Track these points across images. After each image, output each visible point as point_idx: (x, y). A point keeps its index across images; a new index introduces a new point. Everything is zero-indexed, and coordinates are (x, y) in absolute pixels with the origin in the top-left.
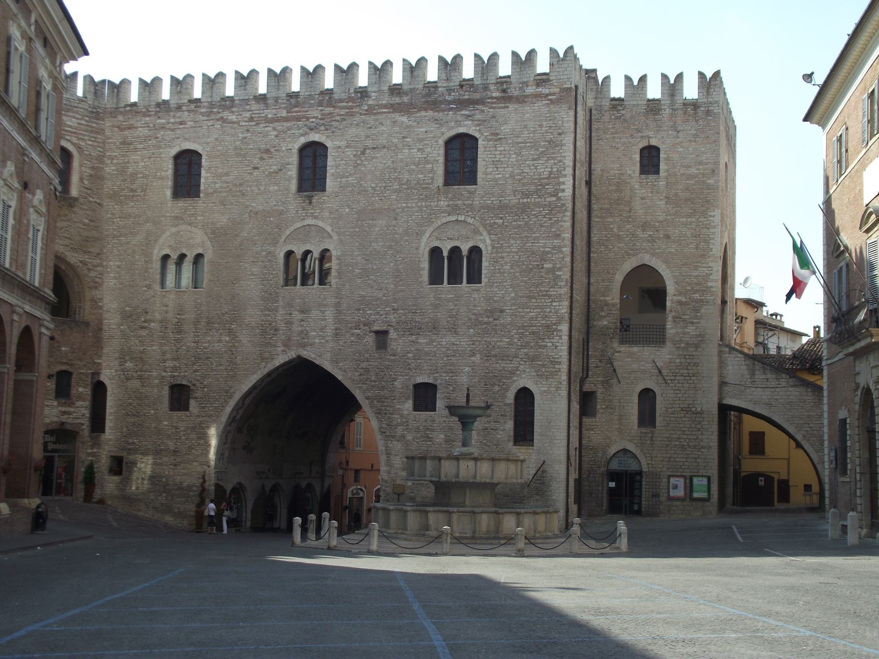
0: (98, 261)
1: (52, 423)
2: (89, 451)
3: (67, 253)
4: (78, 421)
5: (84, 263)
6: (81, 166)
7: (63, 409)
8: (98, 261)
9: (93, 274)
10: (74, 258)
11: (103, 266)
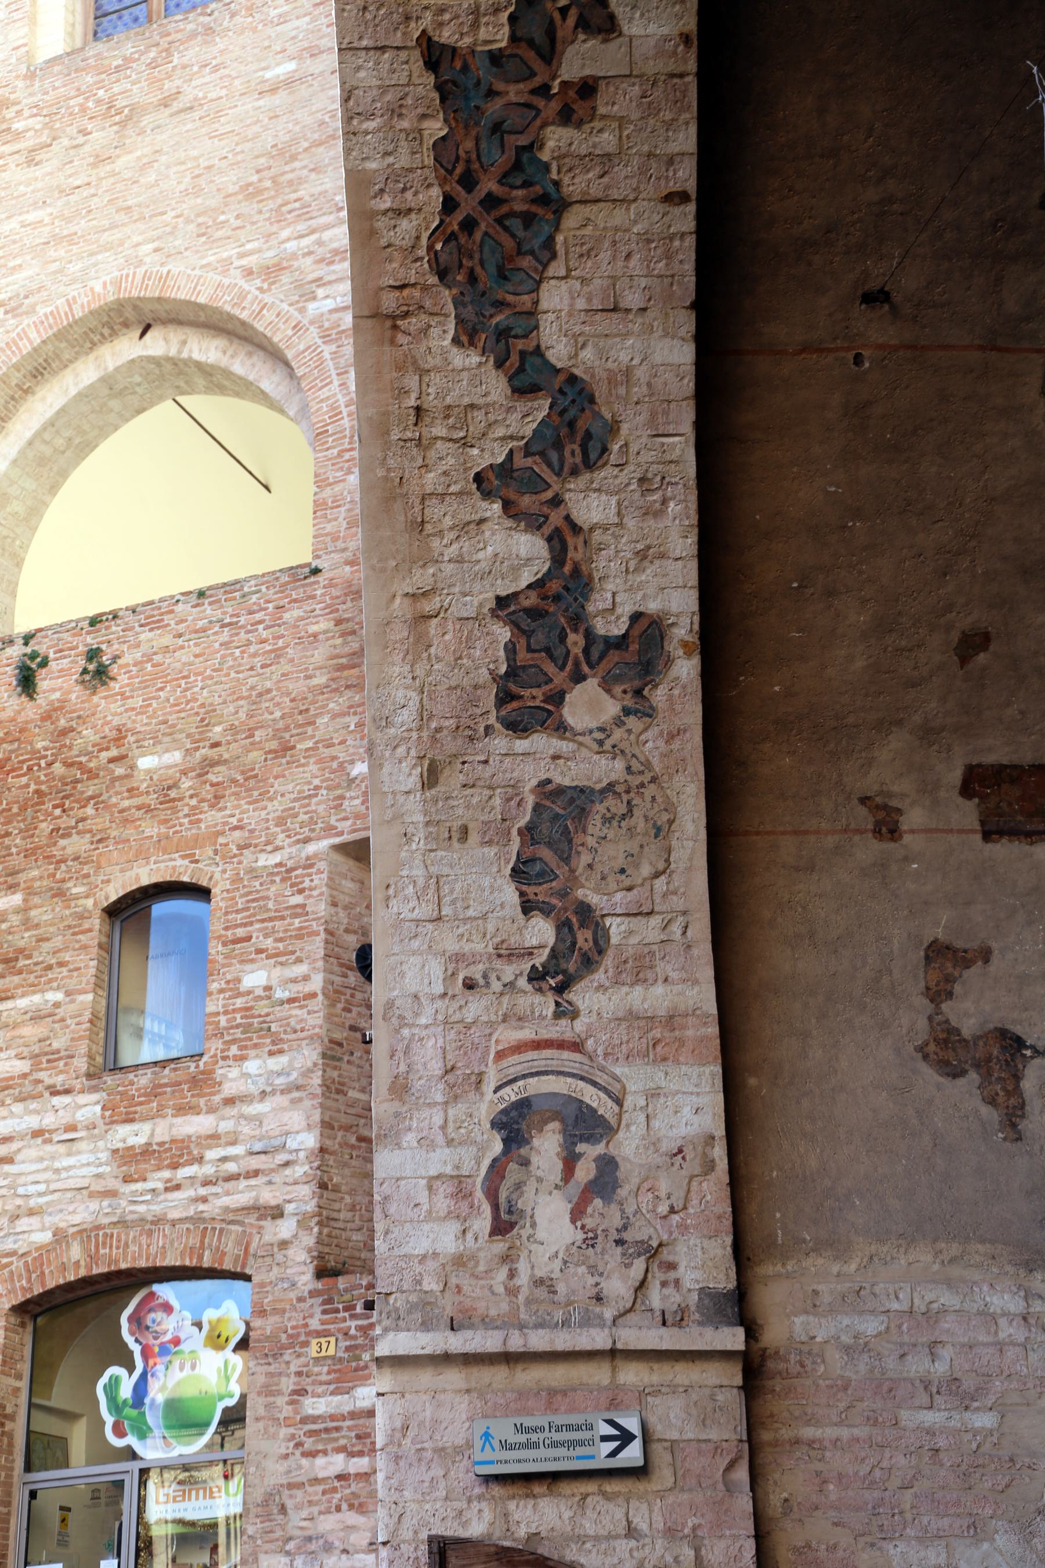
1: (60, 1237)
2: (318, 1405)
3: (175, 267)
4: (242, 1195)
7: (134, 1135)
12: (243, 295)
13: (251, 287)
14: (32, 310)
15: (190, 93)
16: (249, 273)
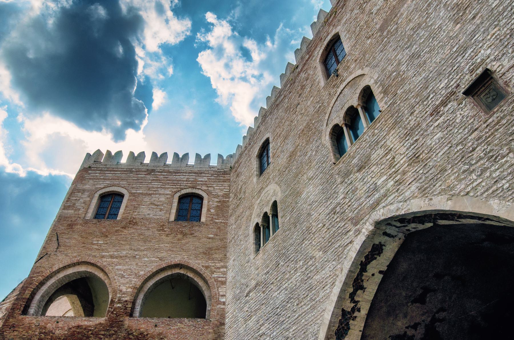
0: (222, 264)
3: (190, 261)
5: (207, 267)
6: (209, 202)
8: (222, 264)
9: (215, 275)
10: (196, 263)
11: (226, 267)
12: (201, 270)
13: (203, 269)
14: (164, 261)
15: (196, 234)
16: (203, 266)
